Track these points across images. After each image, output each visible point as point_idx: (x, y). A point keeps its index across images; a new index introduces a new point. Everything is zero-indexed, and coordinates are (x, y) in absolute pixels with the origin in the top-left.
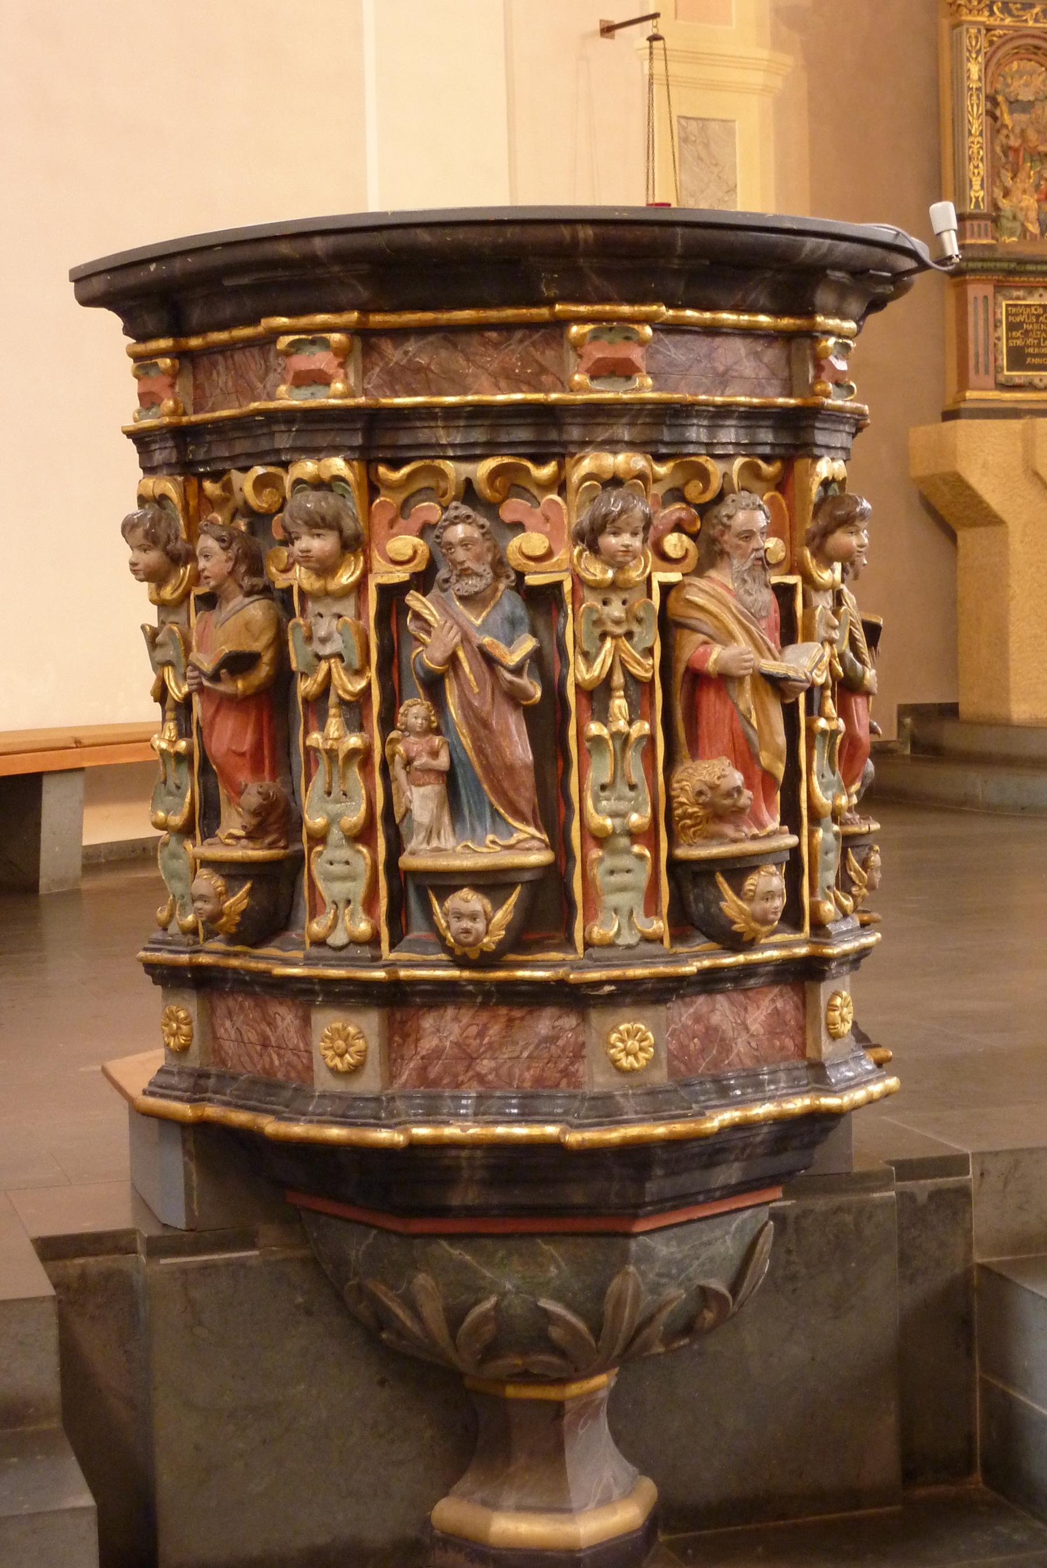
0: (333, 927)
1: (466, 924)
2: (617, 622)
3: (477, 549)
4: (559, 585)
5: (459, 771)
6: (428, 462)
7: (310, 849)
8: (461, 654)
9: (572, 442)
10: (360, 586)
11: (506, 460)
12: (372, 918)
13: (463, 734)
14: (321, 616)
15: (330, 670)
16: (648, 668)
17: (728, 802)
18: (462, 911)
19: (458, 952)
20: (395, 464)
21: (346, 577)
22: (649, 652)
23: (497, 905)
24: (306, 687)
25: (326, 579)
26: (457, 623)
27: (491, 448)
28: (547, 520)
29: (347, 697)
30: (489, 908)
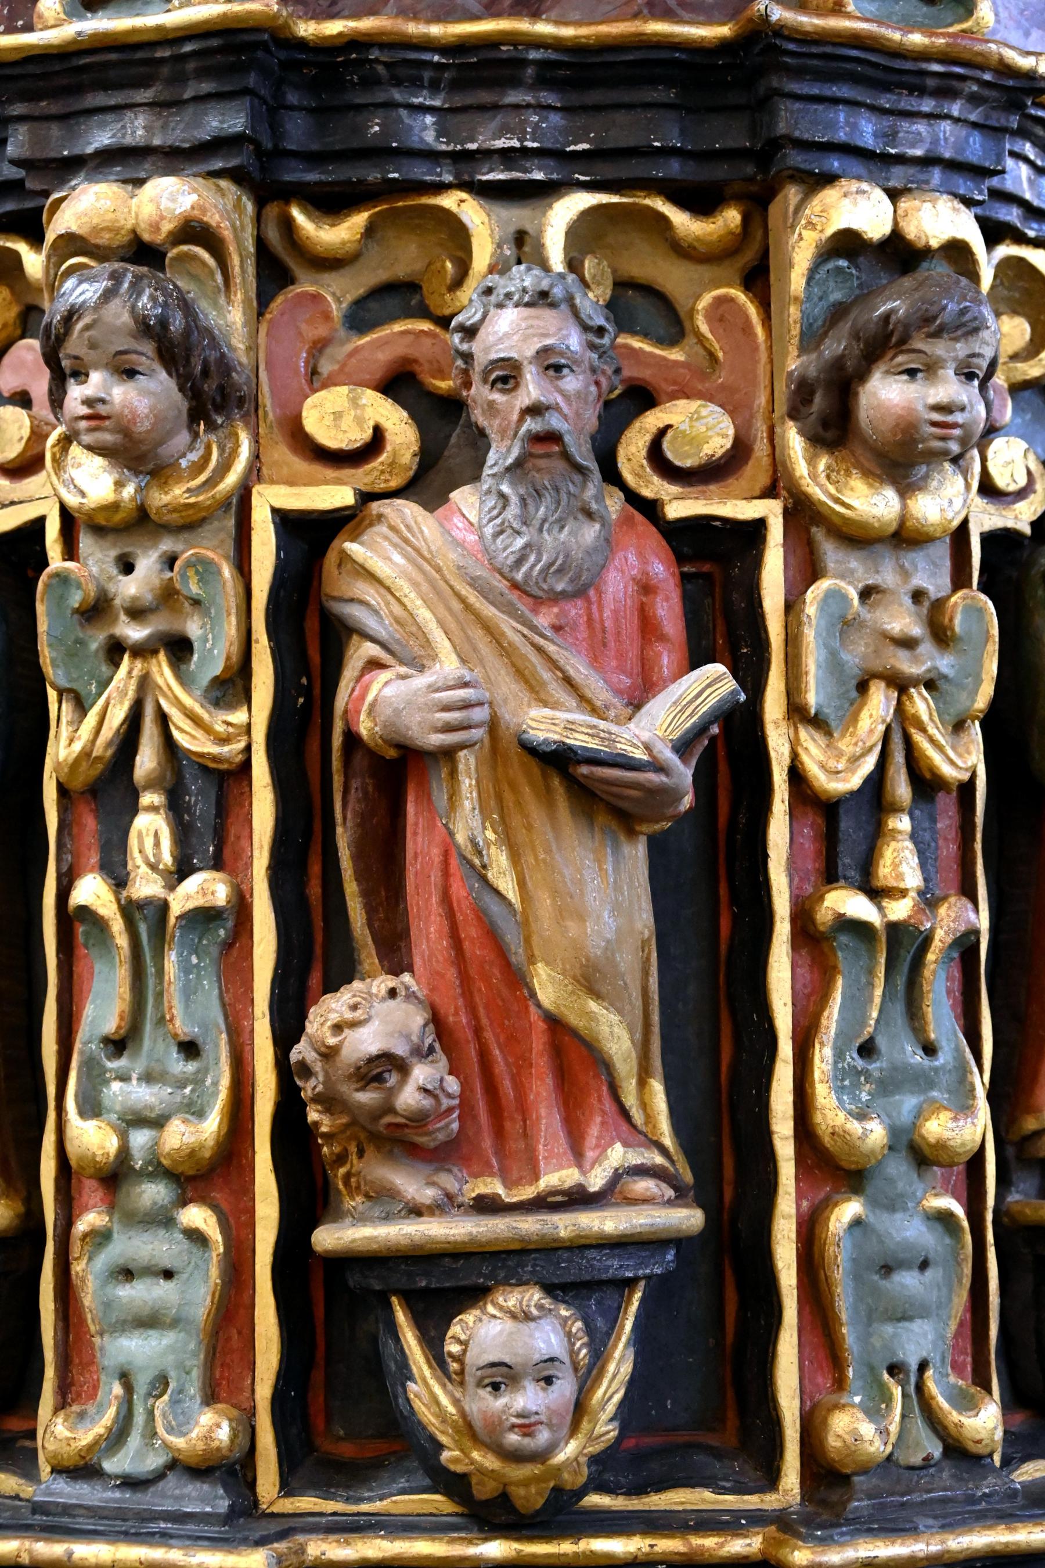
2: (137, 613)
17: (366, 1097)
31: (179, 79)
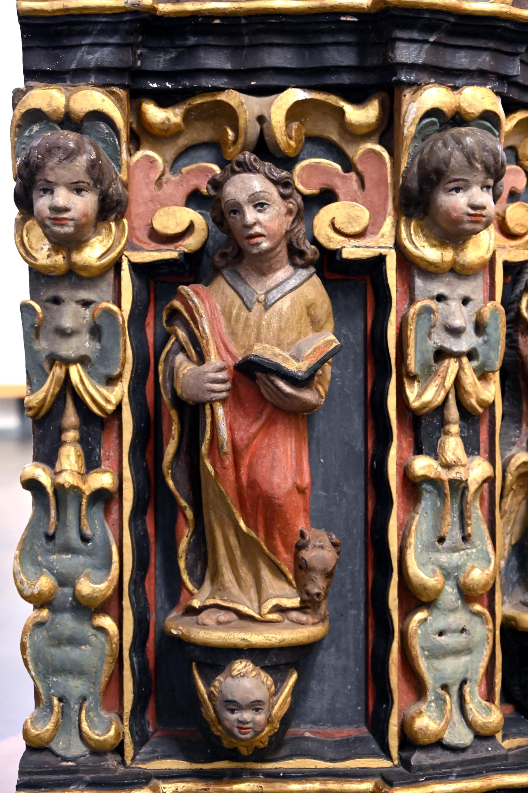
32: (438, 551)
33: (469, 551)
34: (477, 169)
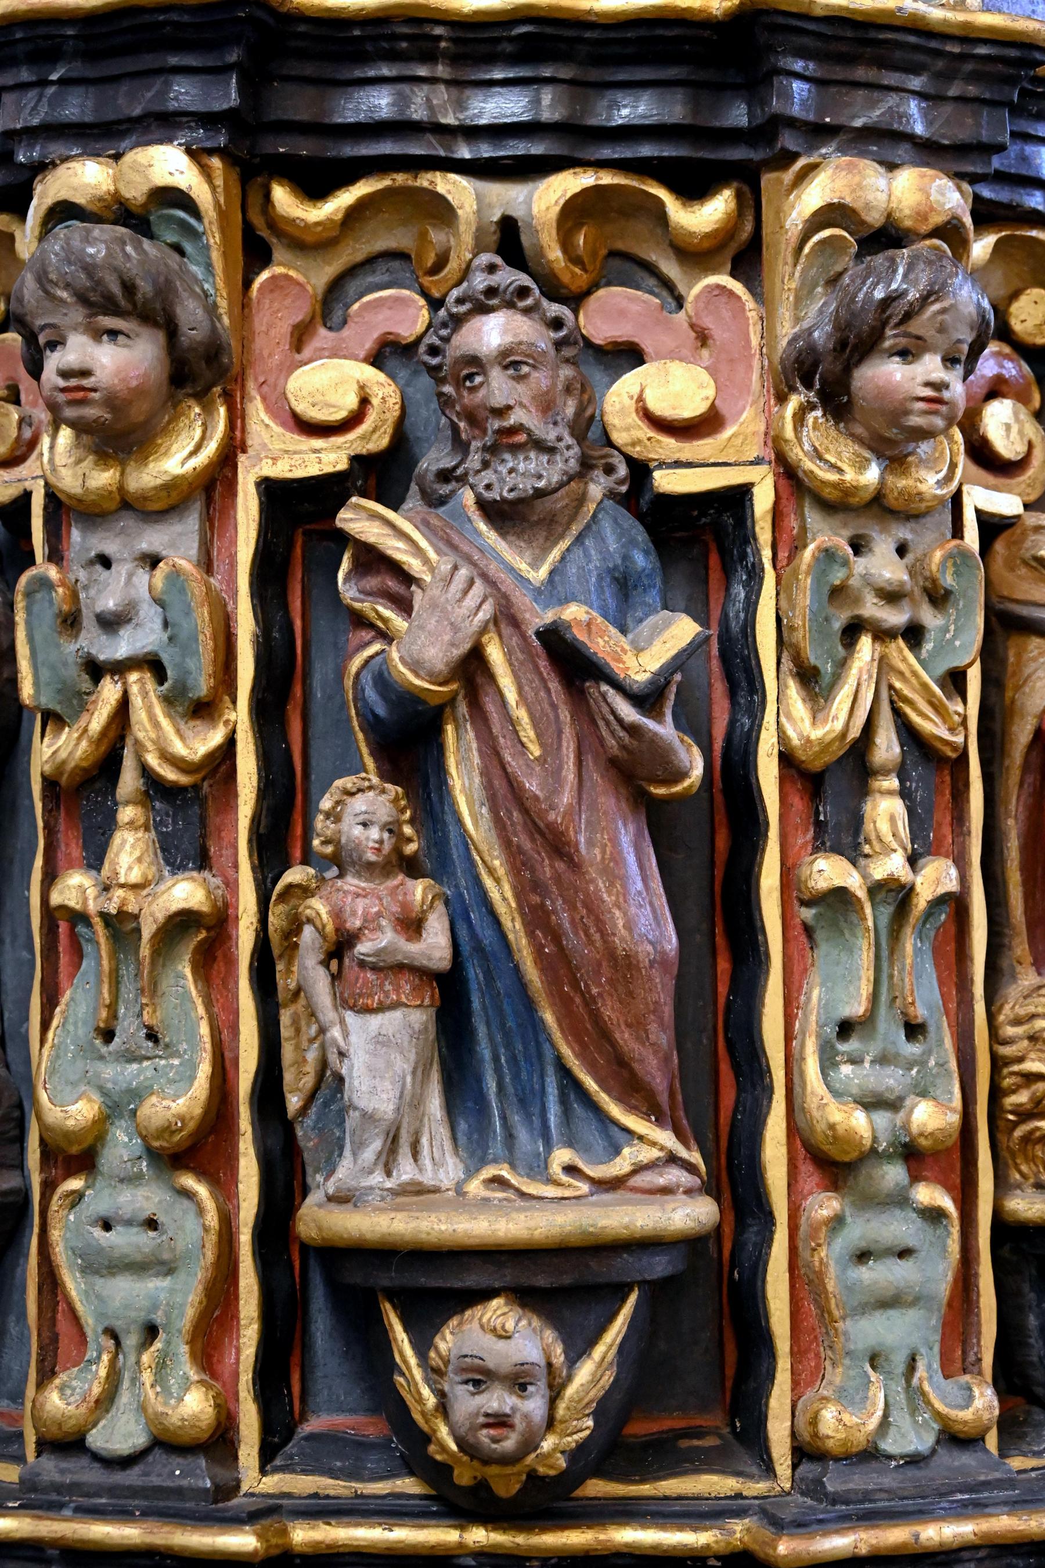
0: (106, 1401)
1: (497, 1400)
2: (891, 596)
3: (540, 379)
4: (738, 497)
5: (474, 973)
6: (401, 179)
7: (49, 1187)
8: (495, 653)
9: (792, 123)
10: (215, 485)
11: (607, 178)
12: (214, 1375)
13: (491, 871)
14: (105, 561)
15: (124, 705)
16: (954, 724)
18: (491, 1363)
19: (463, 1477)
20: (315, 190)
21: (181, 455)
22: (955, 681)
23: (578, 1348)
24: (53, 751)
25: (123, 465)
26: (485, 576)
27: (572, 141)
28: (703, 338)
29: (170, 774)
30: (559, 1356)
31: (946, 76)
32: (102, 1058)
33: (163, 1062)
34: (62, 300)
